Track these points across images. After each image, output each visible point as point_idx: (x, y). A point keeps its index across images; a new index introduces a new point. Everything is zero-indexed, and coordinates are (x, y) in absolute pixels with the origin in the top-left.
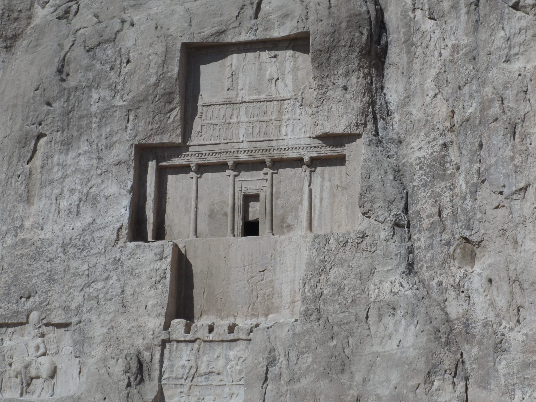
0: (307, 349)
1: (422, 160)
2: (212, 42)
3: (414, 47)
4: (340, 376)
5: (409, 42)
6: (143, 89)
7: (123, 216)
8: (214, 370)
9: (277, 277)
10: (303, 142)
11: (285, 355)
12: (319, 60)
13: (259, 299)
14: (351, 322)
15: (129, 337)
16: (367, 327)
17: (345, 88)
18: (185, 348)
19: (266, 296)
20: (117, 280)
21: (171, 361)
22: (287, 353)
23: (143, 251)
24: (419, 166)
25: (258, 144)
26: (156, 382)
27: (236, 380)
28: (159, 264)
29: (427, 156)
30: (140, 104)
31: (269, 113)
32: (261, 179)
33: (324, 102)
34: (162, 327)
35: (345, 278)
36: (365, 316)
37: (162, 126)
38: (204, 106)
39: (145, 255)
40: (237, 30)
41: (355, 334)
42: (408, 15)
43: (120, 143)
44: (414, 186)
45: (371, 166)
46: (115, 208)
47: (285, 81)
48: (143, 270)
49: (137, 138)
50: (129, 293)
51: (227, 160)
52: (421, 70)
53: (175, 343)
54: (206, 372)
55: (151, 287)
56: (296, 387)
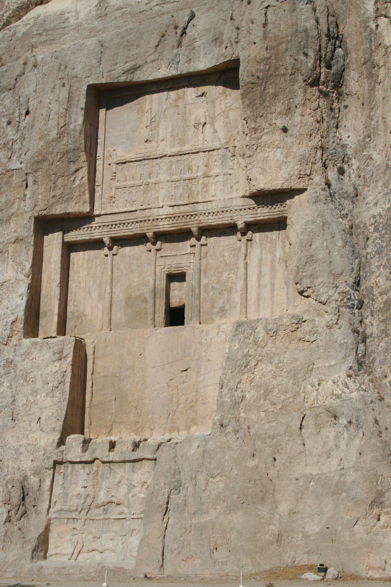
0: (219, 471)
1: (378, 218)
2: (125, 82)
3: (376, 69)
4: (259, 506)
5: (369, 63)
6: (42, 146)
7: (18, 306)
8: (113, 499)
9: (201, 378)
10: (235, 203)
11: (191, 478)
12: (251, 95)
13: (180, 406)
14: (278, 435)
15: (15, 458)
16: (300, 441)
17: (285, 130)
18: (82, 471)
19: (188, 402)
20: (8, 387)
21: (64, 488)
22: (194, 475)
23: (40, 350)
24: (373, 226)
26: (44, 516)
27: (138, 512)
28: (58, 364)
29: (383, 213)
30: (40, 166)
31: (194, 169)
33: (259, 150)
35: (275, 377)
36: (299, 426)
37: (67, 191)
38: (118, 164)
39: (42, 354)
40: (155, 64)
41: (283, 451)
42: (368, 26)
43: (17, 216)
44: (367, 254)
45: (315, 230)
46: (11, 297)
47: (214, 125)
48: (40, 373)
49: (36, 209)
50: (21, 403)
51: (145, 231)
52: (384, 98)
53: (70, 465)
54: (104, 502)
55: (47, 394)
56: (203, 520)
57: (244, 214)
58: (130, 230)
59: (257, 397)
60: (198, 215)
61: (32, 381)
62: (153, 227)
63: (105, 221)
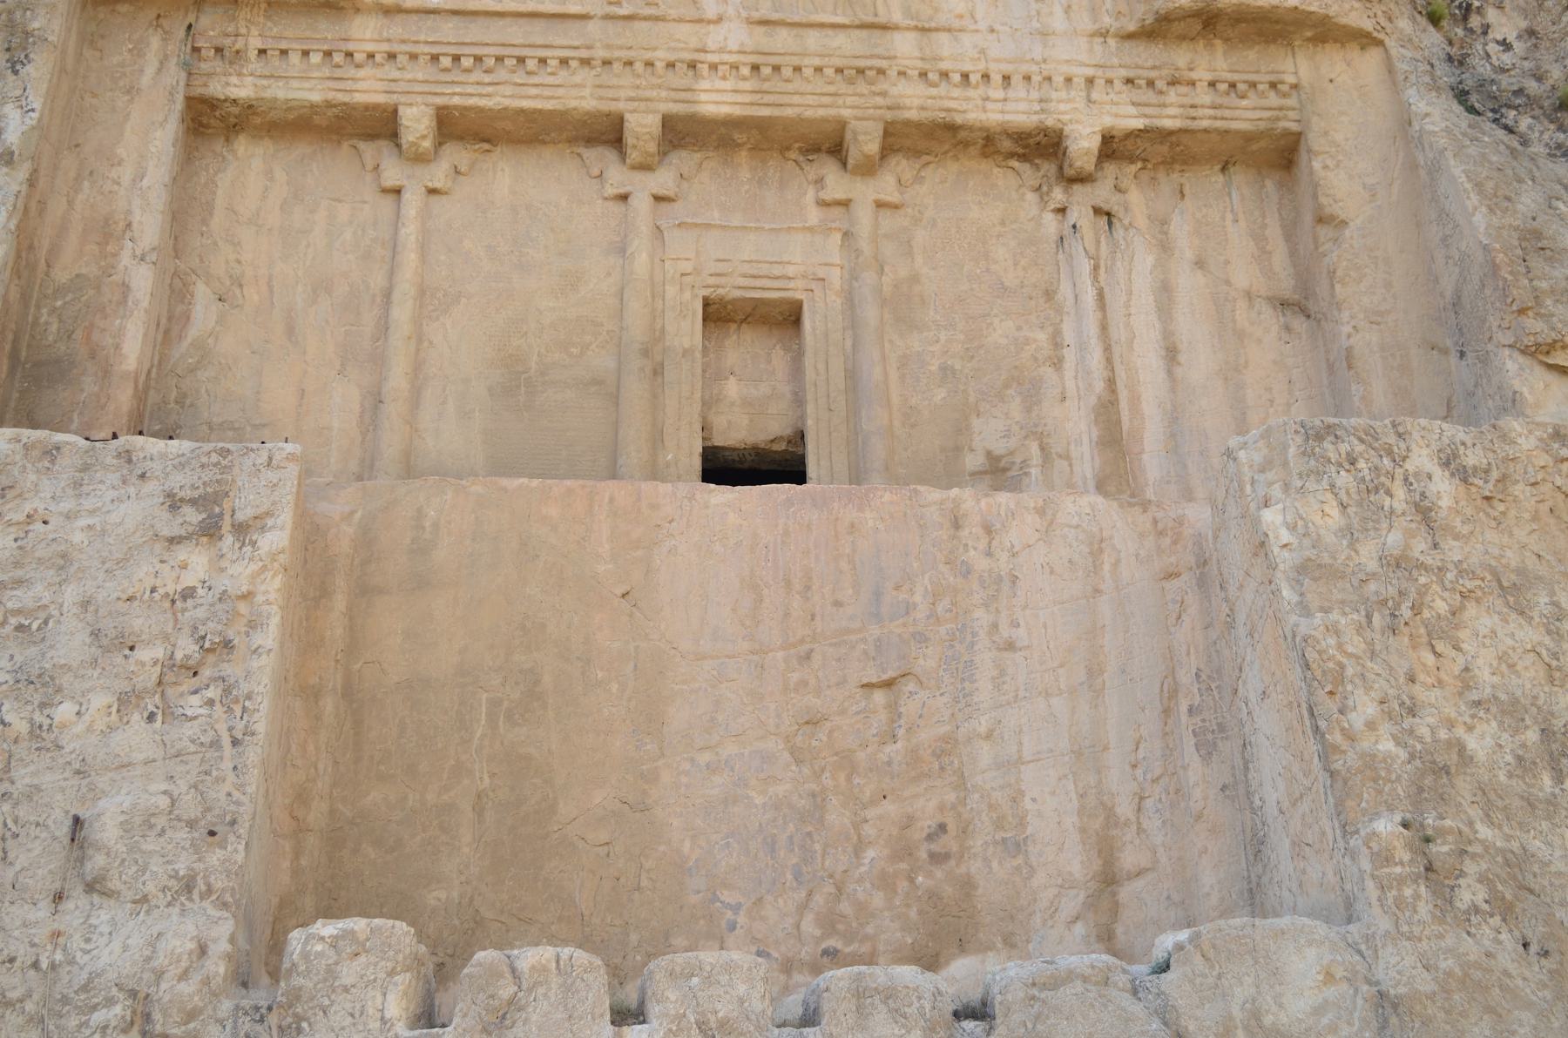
23: (78, 484)
25: (813, 39)
32: (811, 229)
34: (217, 967)
39: (88, 504)
48: (71, 594)
55: (126, 701)
57: (1107, 98)
58: (547, 92)
59: (1520, 759)
60: (893, 73)
61: (20, 628)
62: (664, 94)
63: (422, 38)
